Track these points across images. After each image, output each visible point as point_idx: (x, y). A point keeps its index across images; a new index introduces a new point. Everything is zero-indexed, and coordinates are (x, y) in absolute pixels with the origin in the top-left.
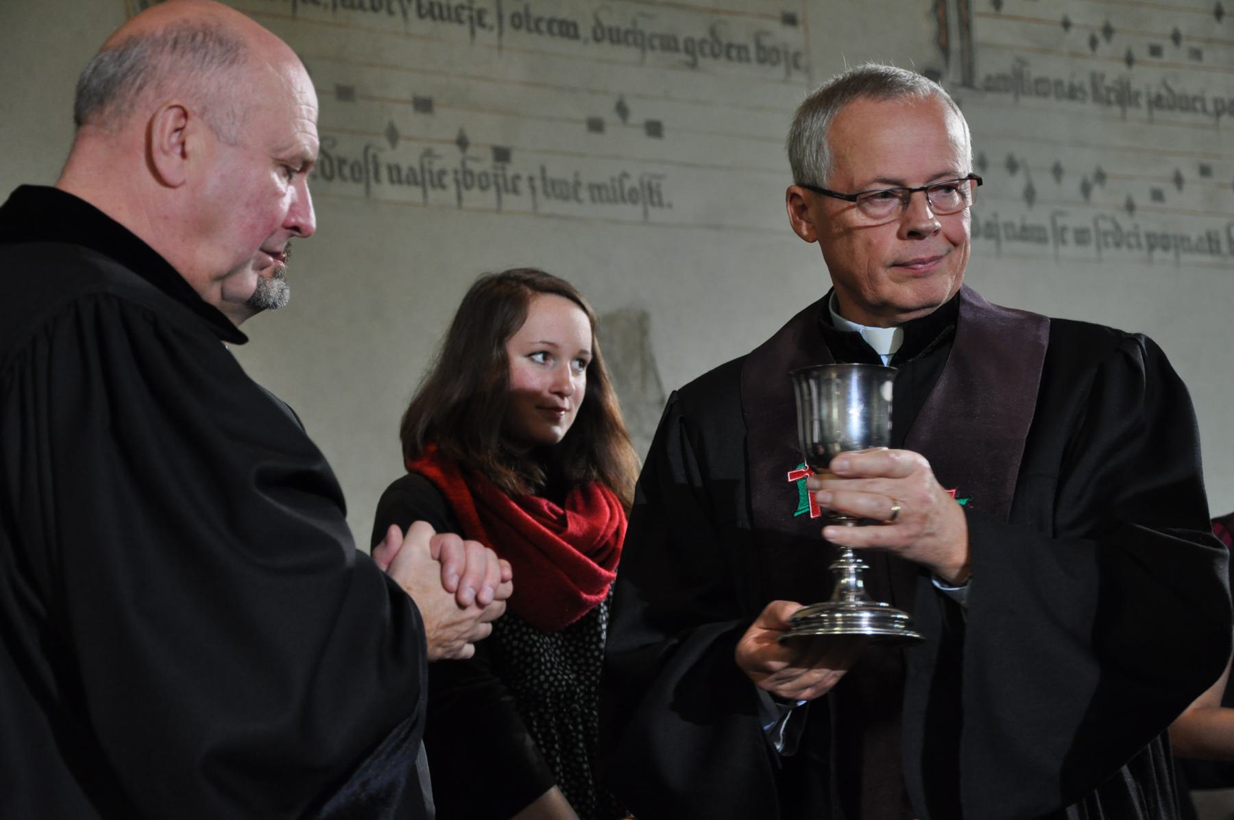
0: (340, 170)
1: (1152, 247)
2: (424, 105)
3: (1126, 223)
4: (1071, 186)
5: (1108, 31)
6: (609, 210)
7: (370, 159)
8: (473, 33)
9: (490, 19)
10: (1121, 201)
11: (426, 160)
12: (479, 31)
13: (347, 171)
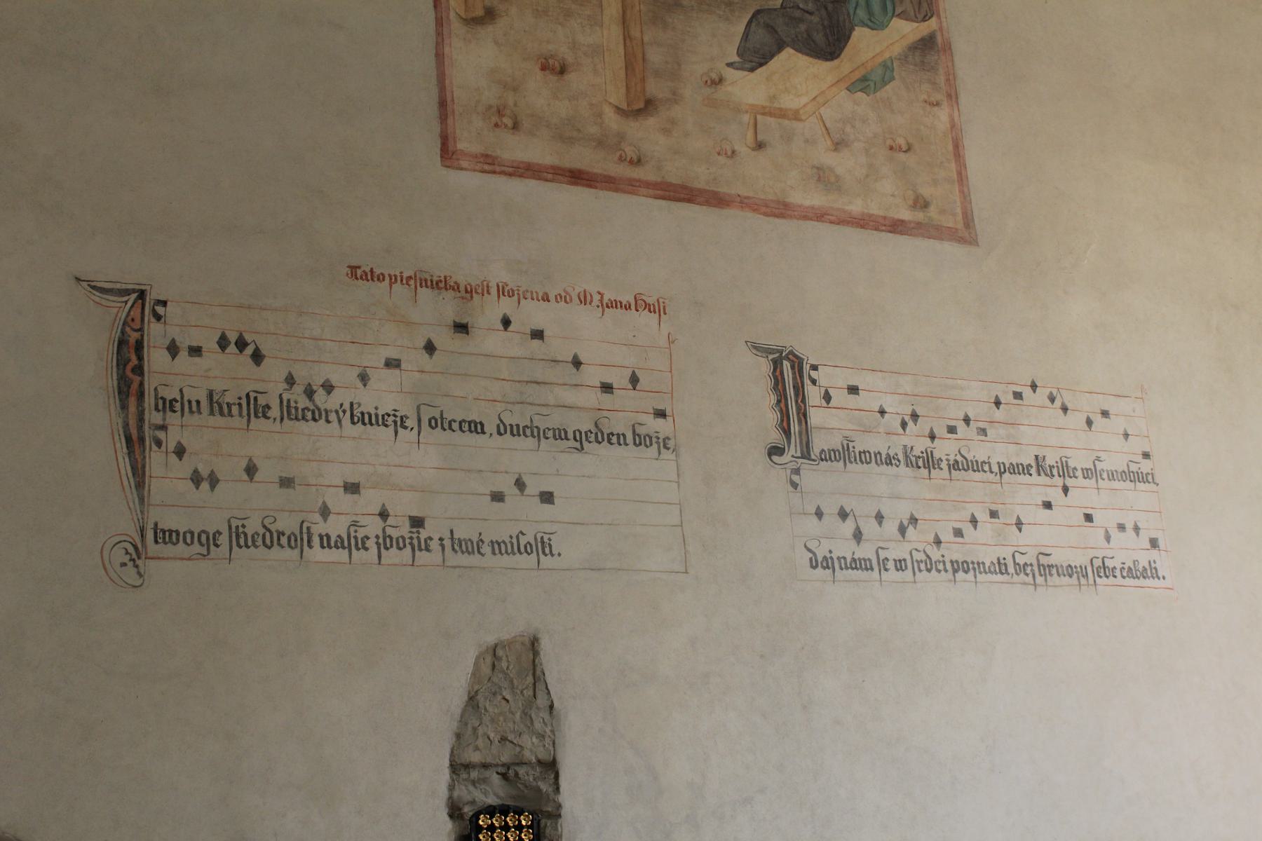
0: (279, 539)
1: (955, 571)
2: (352, 488)
3: (935, 554)
4: (891, 527)
6: (506, 560)
7: (305, 530)
8: (396, 433)
9: (408, 423)
10: (931, 538)
11: (352, 529)
12: (400, 429)
13: (284, 540)
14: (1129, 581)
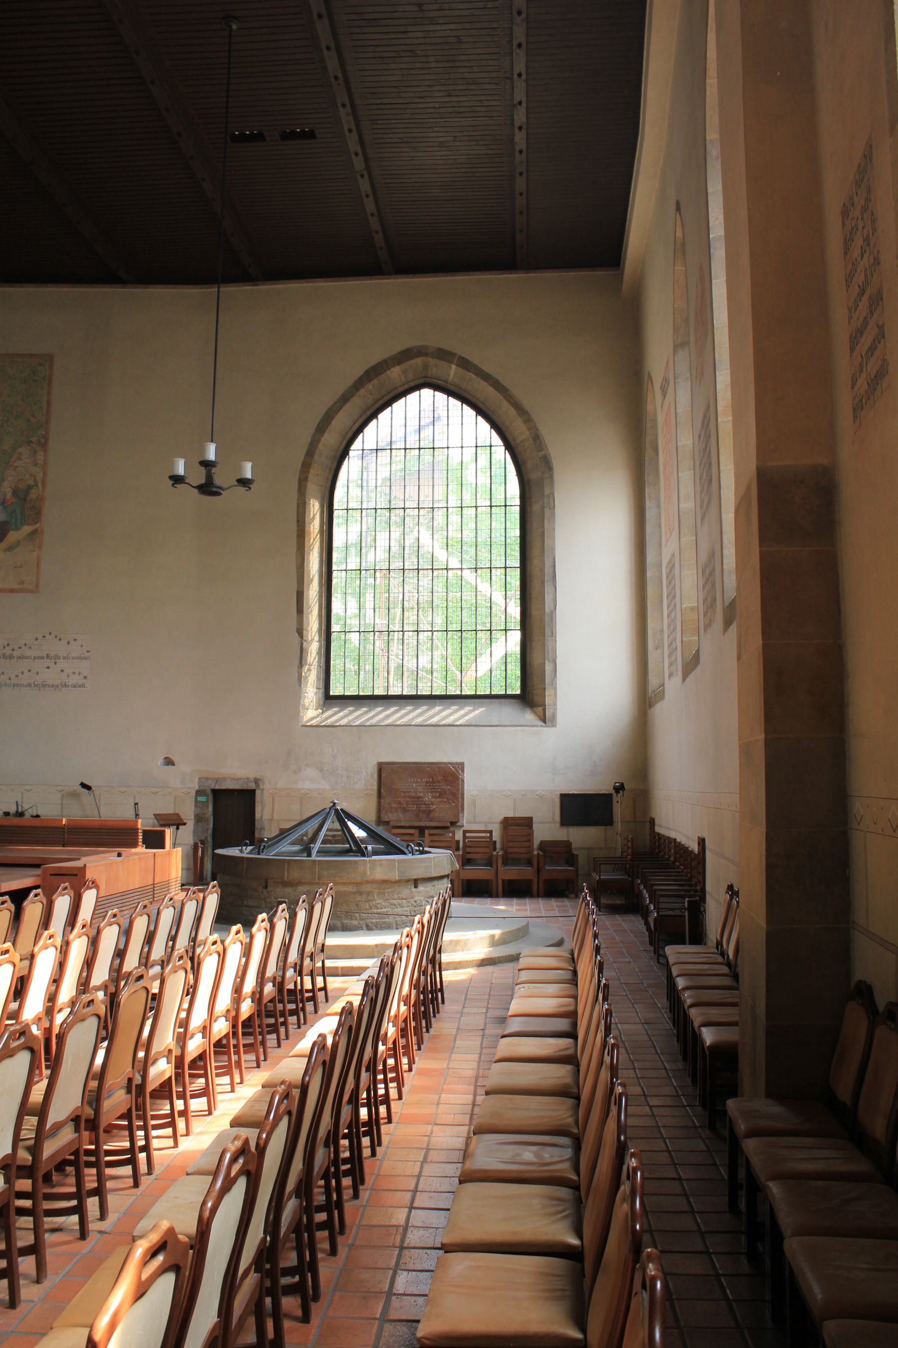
1: (14, 686)
3: (8, 682)
5: (8, 645)
14: (73, 689)
